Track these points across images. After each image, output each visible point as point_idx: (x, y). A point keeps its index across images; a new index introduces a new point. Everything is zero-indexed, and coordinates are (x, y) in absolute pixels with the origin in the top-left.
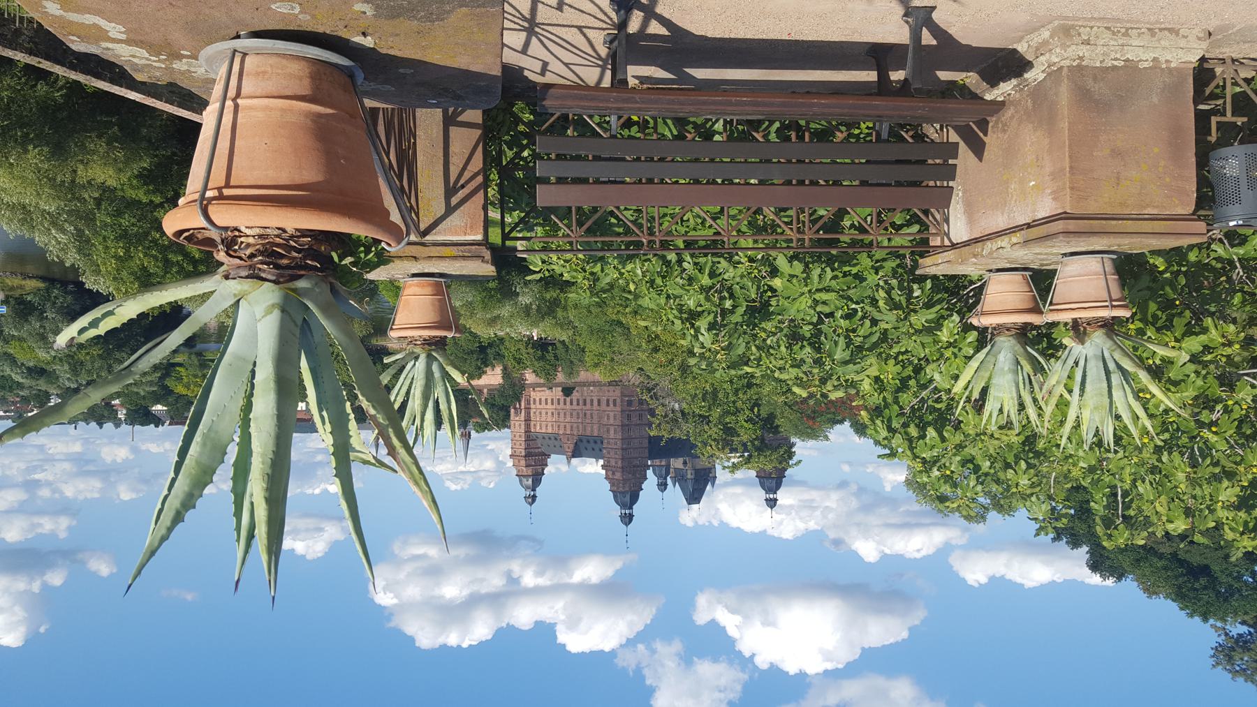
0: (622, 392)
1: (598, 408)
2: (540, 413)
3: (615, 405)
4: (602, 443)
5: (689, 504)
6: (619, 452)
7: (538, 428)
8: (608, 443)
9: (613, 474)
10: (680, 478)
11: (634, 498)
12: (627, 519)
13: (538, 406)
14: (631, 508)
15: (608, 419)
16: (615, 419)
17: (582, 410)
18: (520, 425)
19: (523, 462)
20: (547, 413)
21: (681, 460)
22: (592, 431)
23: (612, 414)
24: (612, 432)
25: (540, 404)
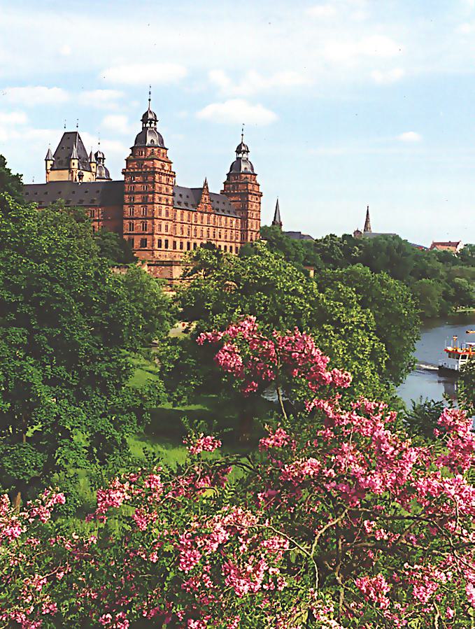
0: (153, 253)
1: (176, 239)
2: (231, 238)
3: (160, 241)
4: (173, 201)
5: (76, 133)
6: (157, 190)
7: (234, 222)
8: (167, 200)
9: (163, 166)
10: (85, 162)
11: (141, 138)
12: (148, 119)
13: (233, 245)
14: (145, 129)
15: (167, 226)
16: (160, 226)
17: (192, 238)
18: (252, 226)
19: (250, 187)
20: (226, 237)
21: (85, 180)
22: (182, 214)
23: (163, 231)
24: (164, 212)
25: (231, 247)
